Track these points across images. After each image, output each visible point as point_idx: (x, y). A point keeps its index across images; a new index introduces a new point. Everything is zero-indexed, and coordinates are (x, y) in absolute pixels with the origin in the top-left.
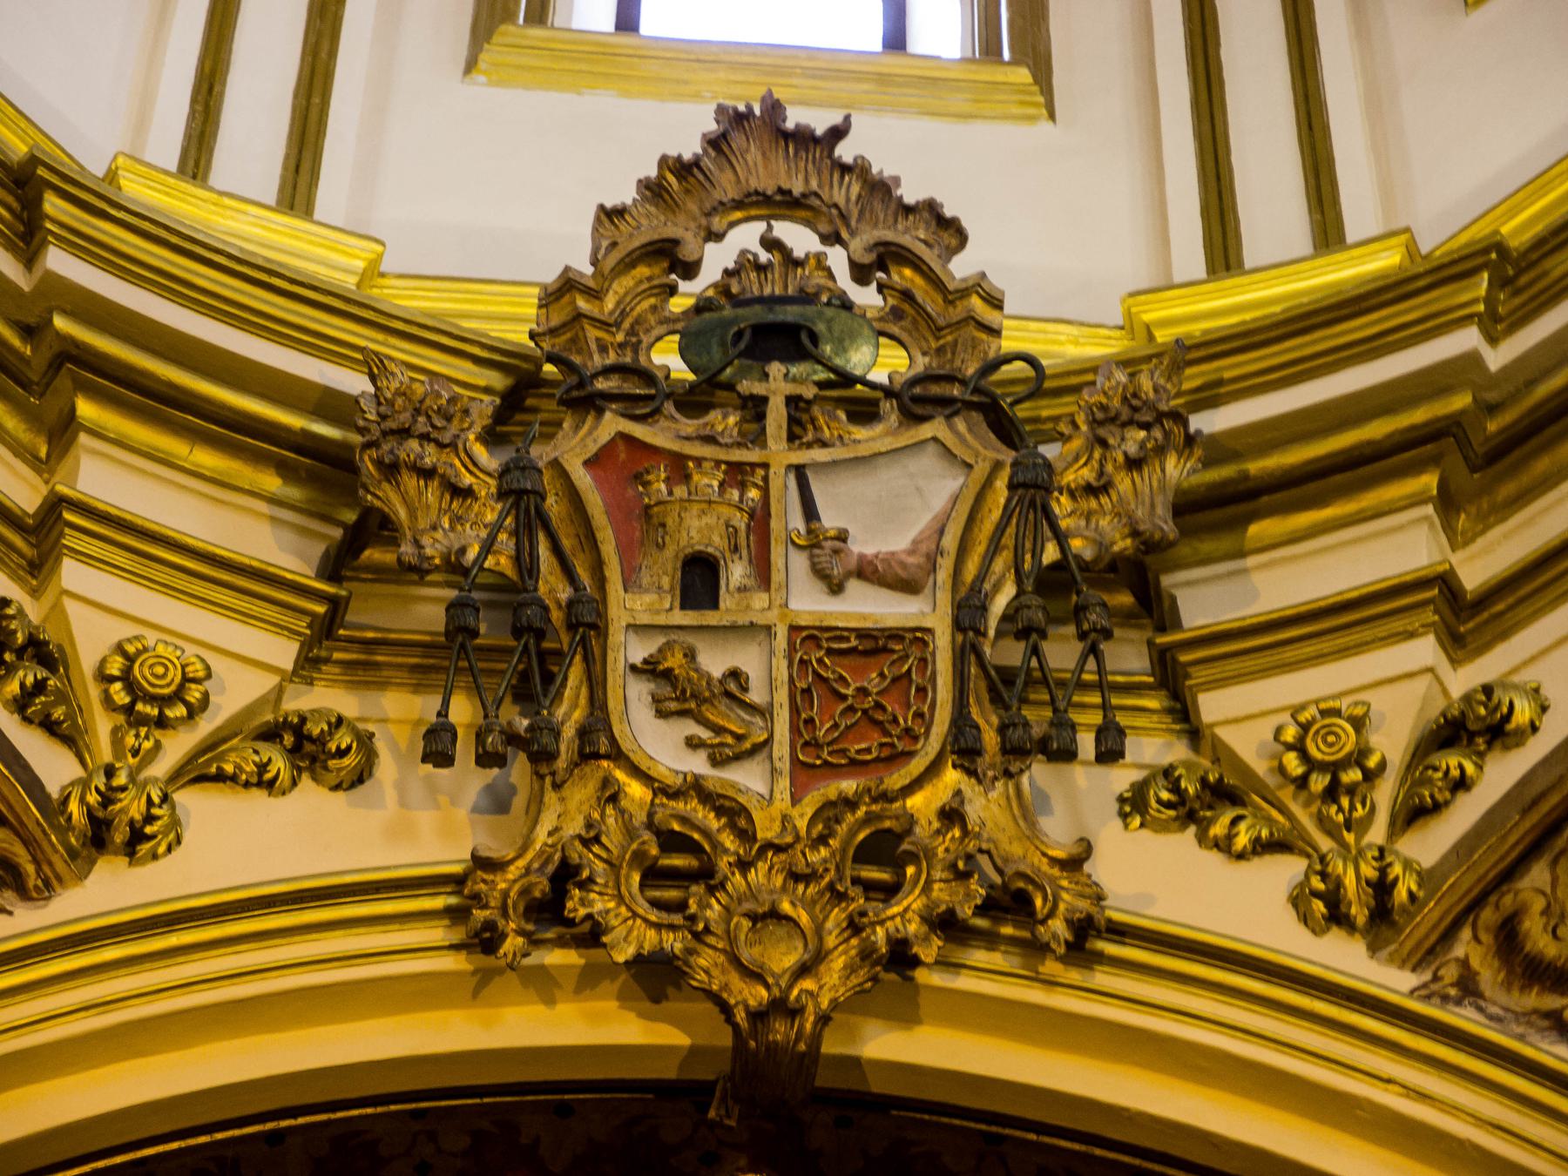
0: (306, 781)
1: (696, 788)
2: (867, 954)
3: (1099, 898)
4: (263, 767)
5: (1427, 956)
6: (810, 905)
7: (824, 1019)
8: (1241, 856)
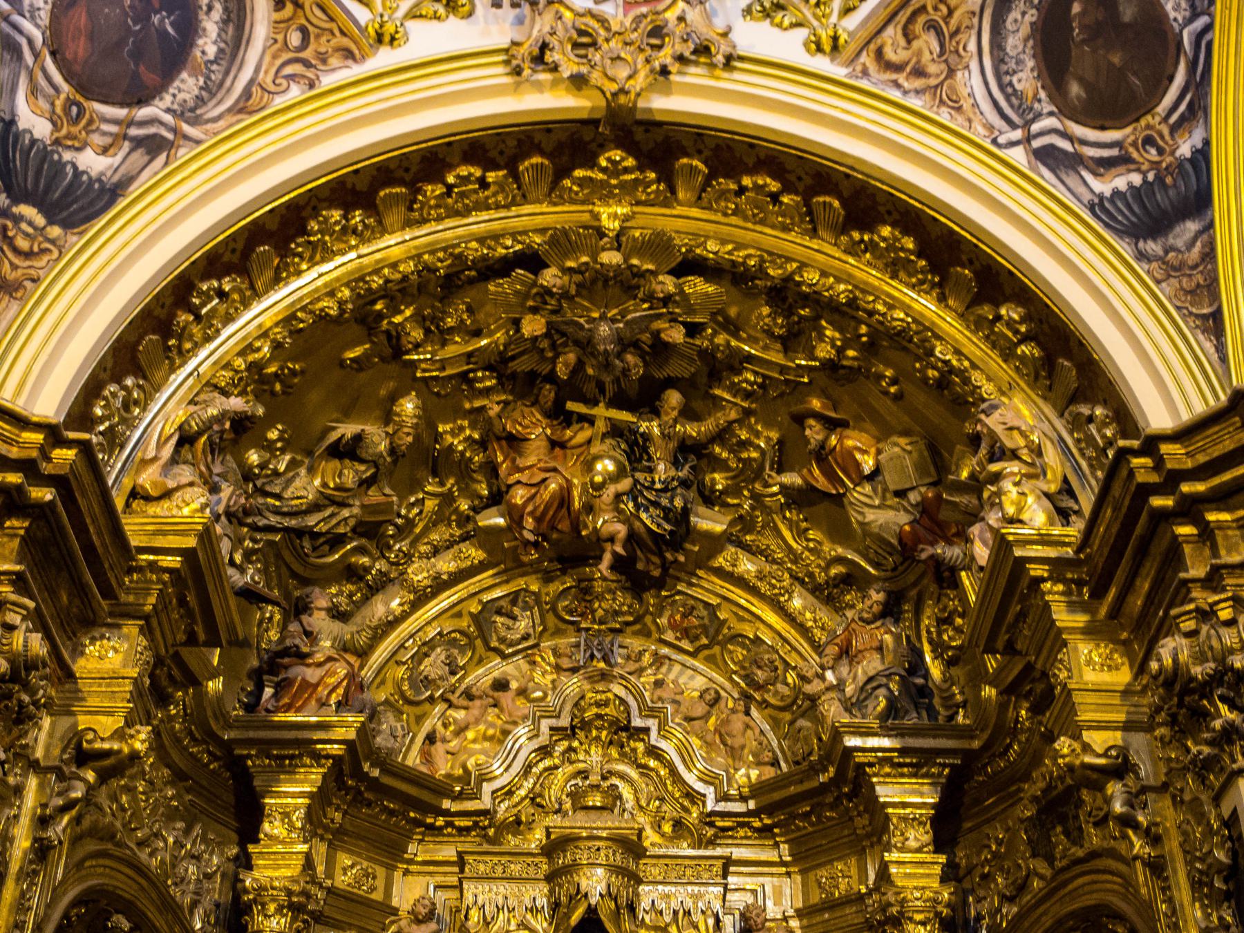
0: (451, 16)
1: (590, 13)
2: (652, 71)
3: (734, 47)
4: (435, 12)
5: (852, 61)
6: (632, 54)
7: (638, 95)
8: (786, 29)
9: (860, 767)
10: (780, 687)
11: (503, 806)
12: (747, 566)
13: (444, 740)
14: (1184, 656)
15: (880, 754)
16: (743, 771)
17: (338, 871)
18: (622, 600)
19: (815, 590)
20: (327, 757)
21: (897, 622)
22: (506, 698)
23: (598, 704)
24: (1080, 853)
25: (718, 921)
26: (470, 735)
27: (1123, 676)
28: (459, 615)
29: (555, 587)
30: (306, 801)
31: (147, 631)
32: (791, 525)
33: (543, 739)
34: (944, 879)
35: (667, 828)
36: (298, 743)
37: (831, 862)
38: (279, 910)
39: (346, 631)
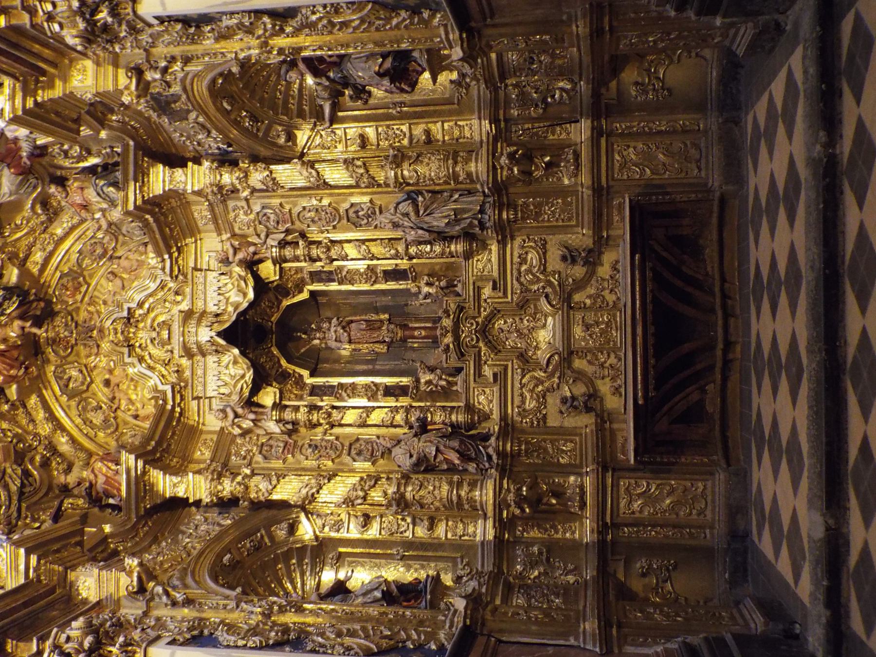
9: (144, 202)
10: (105, 241)
11: (170, 379)
12: (38, 256)
13: (137, 410)
14: (74, 32)
15: (138, 192)
16: (150, 261)
17: (201, 458)
18: (58, 321)
19: (50, 221)
20: (144, 468)
21: (67, 179)
22: (114, 381)
23: (116, 333)
24: (184, 97)
25: (223, 274)
26: (133, 397)
27: (89, 64)
28: (69, 407)
29: (52, 356)
30: (167, 476)
31: (73, 568)
32: (13, 232)
33: (135, 360)
34: (200, 164)
35: (179, 298)
36: (137, 483)
37: (194, 219)
38: (220, 484)
39: (78, 464)
